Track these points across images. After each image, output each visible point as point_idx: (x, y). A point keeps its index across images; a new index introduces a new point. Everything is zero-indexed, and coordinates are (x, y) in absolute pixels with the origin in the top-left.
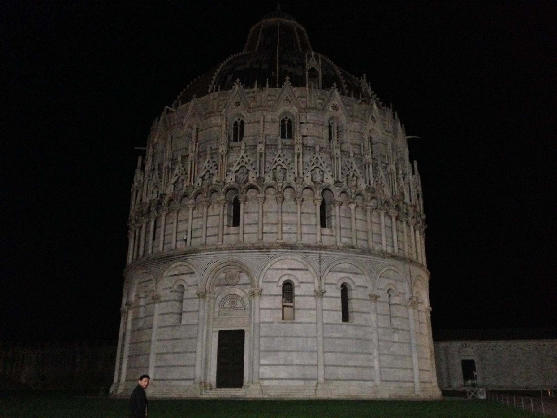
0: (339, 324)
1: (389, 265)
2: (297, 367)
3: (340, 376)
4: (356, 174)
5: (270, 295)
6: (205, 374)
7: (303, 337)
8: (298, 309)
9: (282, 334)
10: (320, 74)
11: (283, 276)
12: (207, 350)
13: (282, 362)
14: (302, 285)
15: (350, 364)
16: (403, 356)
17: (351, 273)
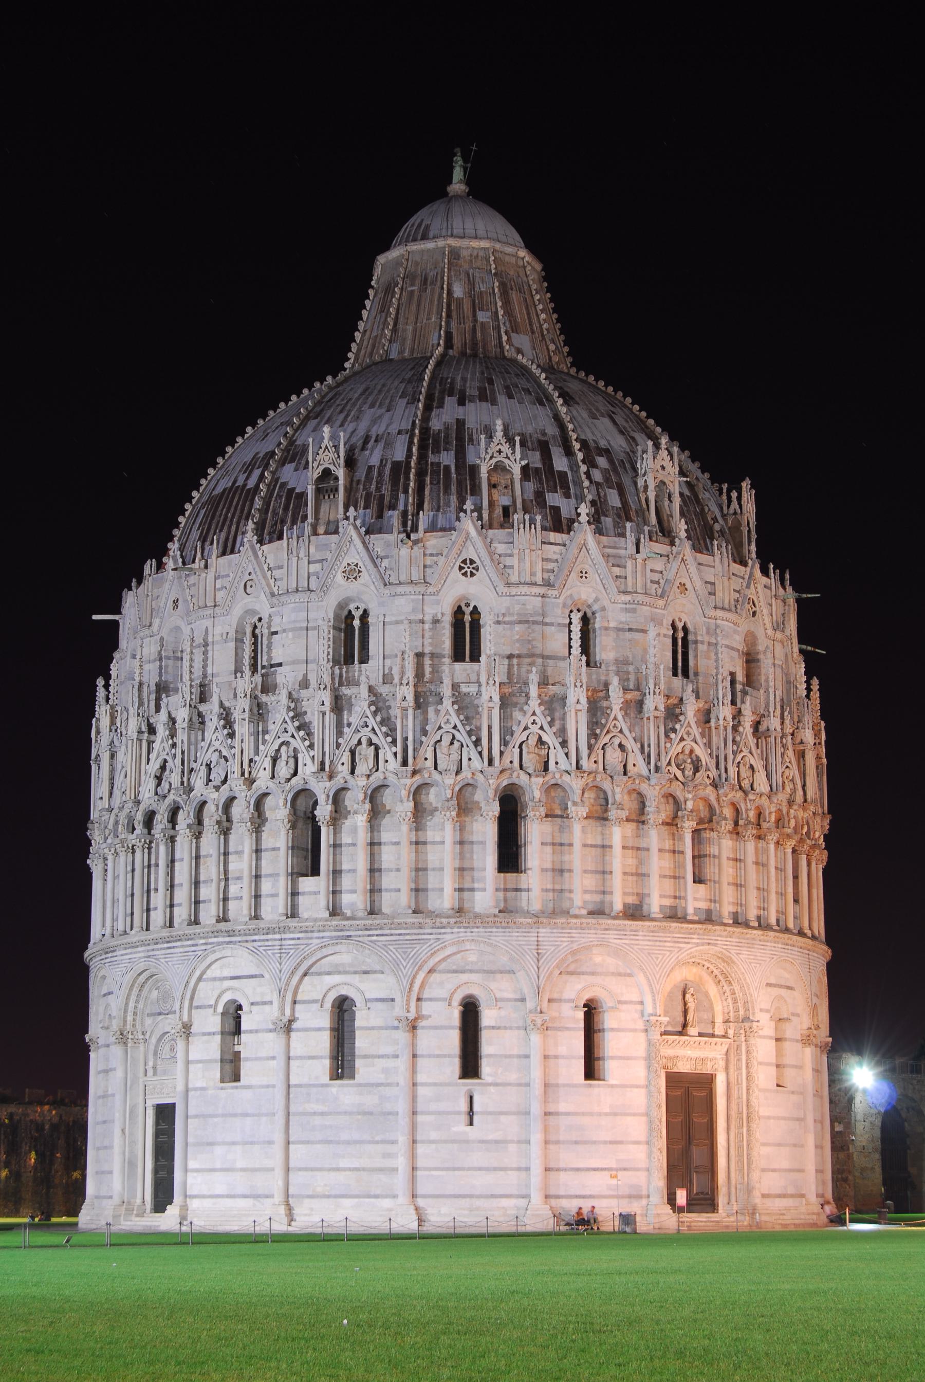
0: (323, 1085)
1: (454, 944)
2: (242, 1173)
3: (319, 1190)
4: (375, 740)
5: (204, 1034)
6: (132, 1190)
7: (254, 1115)
8: (247, 1059)
9: (220, 1111)
10: (341, 482)
11: (223, 992)
12: (133, 1143)
13: (218, 1166)
14: (255, 1009)
15: (343, 1163)
16: (496, 1142)
17: (355, 973)
